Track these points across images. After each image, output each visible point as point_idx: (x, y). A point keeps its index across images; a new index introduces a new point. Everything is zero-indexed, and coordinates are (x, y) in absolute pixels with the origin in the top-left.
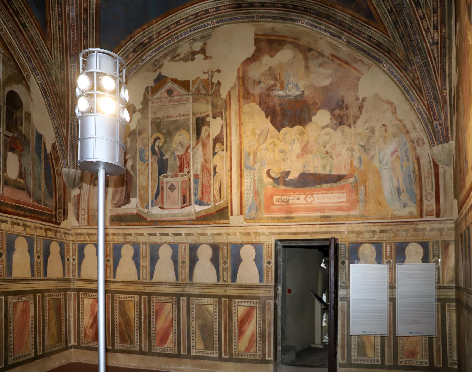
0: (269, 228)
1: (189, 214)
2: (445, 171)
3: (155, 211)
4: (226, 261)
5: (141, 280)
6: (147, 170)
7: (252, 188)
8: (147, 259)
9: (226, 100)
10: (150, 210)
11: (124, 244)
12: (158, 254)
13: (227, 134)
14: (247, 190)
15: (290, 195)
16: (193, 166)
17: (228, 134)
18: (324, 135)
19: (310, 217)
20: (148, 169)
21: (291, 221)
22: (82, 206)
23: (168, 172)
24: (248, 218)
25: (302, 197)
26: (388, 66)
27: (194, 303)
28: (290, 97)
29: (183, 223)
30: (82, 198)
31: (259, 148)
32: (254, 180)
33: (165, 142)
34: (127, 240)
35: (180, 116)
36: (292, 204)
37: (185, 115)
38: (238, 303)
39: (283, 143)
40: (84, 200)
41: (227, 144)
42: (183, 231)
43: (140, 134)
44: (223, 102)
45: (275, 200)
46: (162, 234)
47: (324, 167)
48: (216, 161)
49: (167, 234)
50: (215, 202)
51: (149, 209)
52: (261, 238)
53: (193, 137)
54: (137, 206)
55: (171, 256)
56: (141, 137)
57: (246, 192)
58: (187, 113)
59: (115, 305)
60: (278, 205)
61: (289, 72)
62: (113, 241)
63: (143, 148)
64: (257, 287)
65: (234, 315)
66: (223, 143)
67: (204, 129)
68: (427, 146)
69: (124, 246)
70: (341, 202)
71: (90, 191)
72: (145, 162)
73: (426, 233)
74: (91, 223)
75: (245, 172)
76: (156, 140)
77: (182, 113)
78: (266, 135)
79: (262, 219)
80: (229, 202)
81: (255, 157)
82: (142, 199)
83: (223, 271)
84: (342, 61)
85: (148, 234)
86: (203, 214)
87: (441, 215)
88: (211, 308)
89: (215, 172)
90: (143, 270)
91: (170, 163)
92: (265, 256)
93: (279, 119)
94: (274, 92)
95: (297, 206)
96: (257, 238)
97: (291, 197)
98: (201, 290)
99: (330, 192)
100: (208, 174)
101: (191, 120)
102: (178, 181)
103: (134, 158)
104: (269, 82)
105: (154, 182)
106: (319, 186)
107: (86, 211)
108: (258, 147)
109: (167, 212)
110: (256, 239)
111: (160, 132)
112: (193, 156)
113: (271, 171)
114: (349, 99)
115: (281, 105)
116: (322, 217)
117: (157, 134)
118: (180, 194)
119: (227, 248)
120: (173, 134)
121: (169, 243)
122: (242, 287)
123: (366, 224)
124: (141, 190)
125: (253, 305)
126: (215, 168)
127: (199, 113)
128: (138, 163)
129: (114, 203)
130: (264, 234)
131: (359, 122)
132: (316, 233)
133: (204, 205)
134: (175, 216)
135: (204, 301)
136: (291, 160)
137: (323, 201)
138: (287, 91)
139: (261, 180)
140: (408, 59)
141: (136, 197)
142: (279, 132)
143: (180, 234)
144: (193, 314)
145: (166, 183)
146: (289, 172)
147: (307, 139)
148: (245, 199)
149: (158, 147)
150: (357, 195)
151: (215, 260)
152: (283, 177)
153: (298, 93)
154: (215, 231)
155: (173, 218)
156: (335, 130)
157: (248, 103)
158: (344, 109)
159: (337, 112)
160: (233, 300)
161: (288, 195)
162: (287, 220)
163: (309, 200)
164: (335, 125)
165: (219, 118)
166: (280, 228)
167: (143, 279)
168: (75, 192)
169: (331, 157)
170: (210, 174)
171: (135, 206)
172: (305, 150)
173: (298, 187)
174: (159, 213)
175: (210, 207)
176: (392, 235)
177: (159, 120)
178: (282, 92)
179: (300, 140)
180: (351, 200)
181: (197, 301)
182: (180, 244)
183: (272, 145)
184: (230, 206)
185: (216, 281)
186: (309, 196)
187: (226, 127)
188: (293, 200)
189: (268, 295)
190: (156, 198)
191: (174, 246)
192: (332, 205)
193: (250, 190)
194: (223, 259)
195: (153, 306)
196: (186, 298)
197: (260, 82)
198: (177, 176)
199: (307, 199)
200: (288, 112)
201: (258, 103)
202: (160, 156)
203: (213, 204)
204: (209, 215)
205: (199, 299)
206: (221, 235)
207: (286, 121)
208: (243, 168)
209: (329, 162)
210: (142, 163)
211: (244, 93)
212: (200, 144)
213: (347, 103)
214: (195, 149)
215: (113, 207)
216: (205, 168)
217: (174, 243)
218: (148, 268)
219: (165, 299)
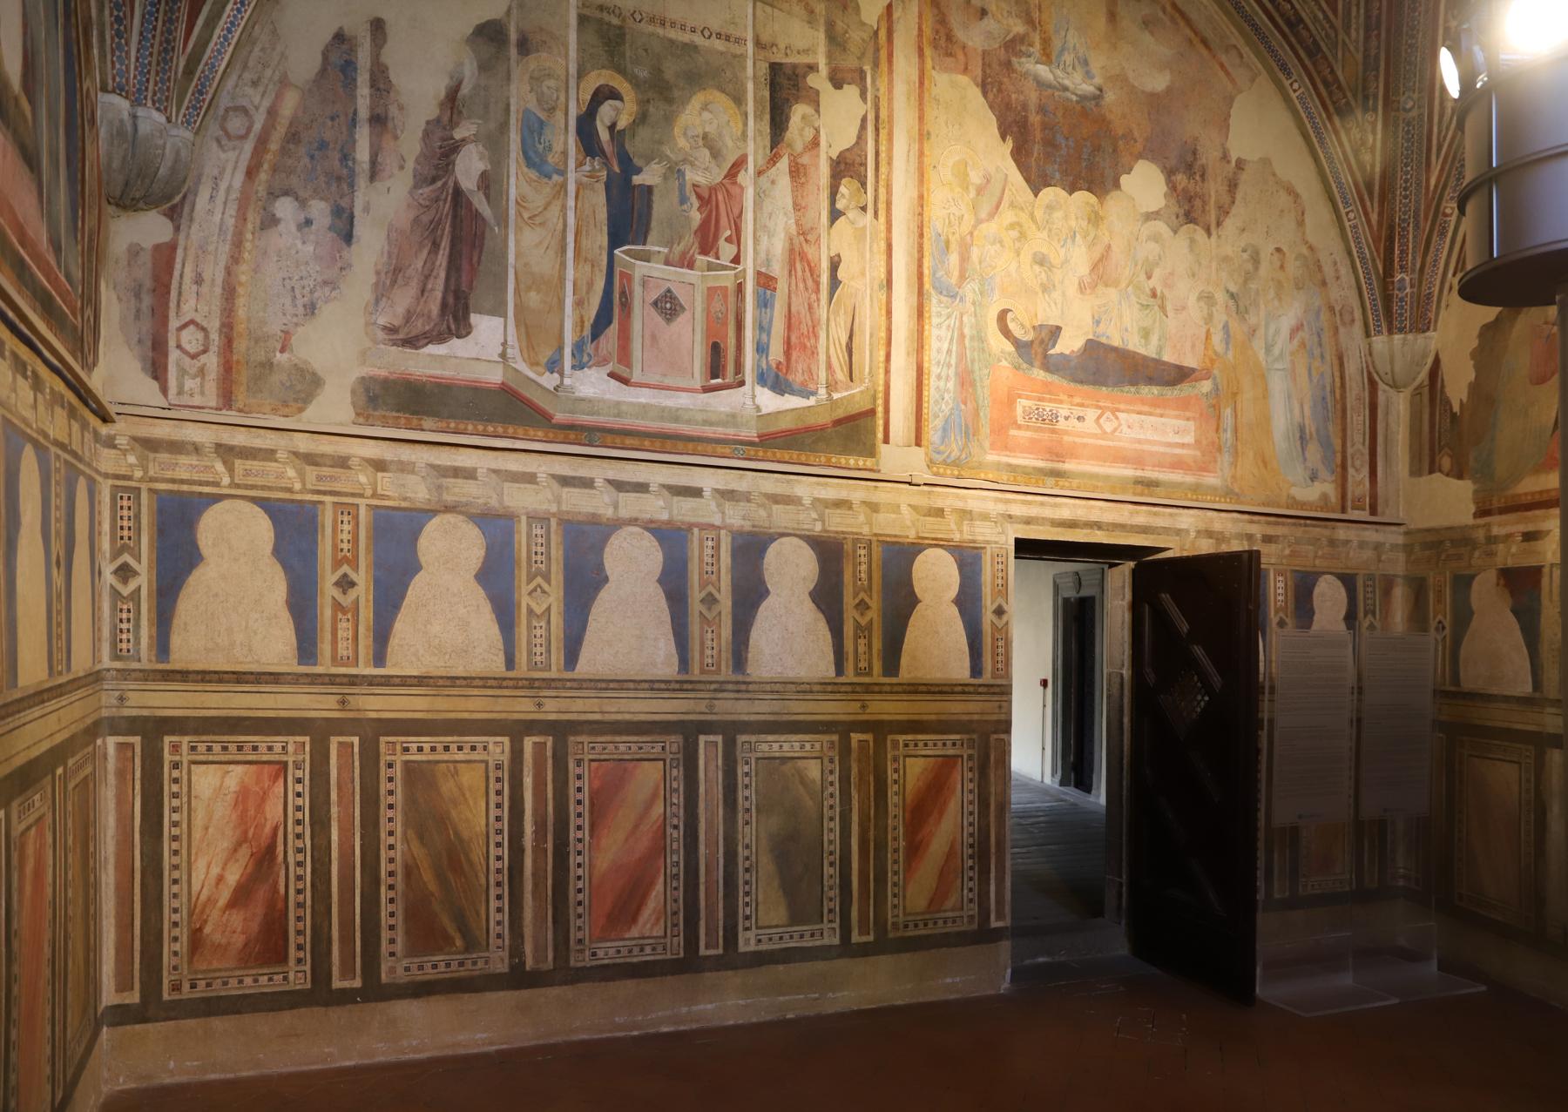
0: (1001, 500)
1: (732, 419)
2: (1388, 400)
3: (592, 385)
4: (867, 599)
5: (522, 670)
6: (555, 210)
7: (953, 362)
8: (549, 582)
9: (876, 33)
10: (567, 381)
11: (434, 513)
12: (600, 567)
13: (877, 154)
14: (939, 362)
15: (1061, 402)
17: (883, 155)
18: (1149, 238)
19: (1107, 478)
20: (564, 208)
21: (1061, 483)
22: (185, 307)
23: (650, 239)
24: (940, 458)
25: (1091, 414)
26: (1302, 90)
27: (753, 756)
28: (1068, 94)
29: (709, 448)
30: (184, 269)
31: (976, 233)
32: (962, 336)
33: (642, 119)
34: (449, 498)
35: (706, 32)
36: (1066, 432)
37: (728, 38)
38: (906, 745)
39: (1045, 234)
40: (199, 280)
41: (876, 190)
42: (708, 481)
43: (524, 46)
44: (865, 36)
45: (1019, 410)
46: (619, 486)
47: (1146, 334)
48: (839, 240)
49: (642, 488)
50: (831, 386)
51: (562, 375)
52: (977, 530)
53: (759, 132)
54: (503, 355)
55: (657, 575)
56: (532, 62)
57: (935, 370)
58: (732, 31)
59: (384, 787)
60: (1028, 428)
61: (1065, 11)
62: (375, 495)
63: (542, 116)
64: (964, 693)
65: (892, 789)
66: (864, 184)
67: (799, 112)
68: (1358, 329)
69: (433, 527)
70: (1183, 445)
71: (238, 244)
72: (550, 178)
73: (1351, 554)
74: (241, 397)
75: (934, 301)
76: (604, 94)
77: (715, 25)
78: (998, 194)
79: (980, 466)
80: (880, 395)
81: (964, 259)
82: (531, 330)
83: (857, 637)
84: (1196, 33)
85: (554, 476)
86: (785, 424)
87: (1380, 509)
88: (813, 770)
89: (835, 283)
90: (530, 628)
91: (660, 207)
92: (987, 591)
93: (1035, 155)
94: (1023, 60)
95: (1078, 440)
96: (965, 528)
97: (1063, 411)
98: (777, 706)
99: (1158, 411)
100: (810, 283)
101: (750, 63)
102: (693, 284)
103: (495, 144)
104: (1011, 21)
105: (588, 268)
106: (1133, 389)
107: (215, 336)
108: (975, 227)
109: (643, 400)
110: (961, 532)
111: (621, 71)
112: (758, 205)
113: (1010, 315)
114: (1209, 155)
115: (1042, 109)
116: (1139, 482)
117: (604, 72)
118: (699, 337)
119: (870, 555)
120: (676, 93)
121: (652, 521)
122: (916, 692)
123: (1235, 515)
124: (529, 289)
125: (951, 752)
126: (835, 265)
127: (782, 46)
128: (513, 170)
129: (382, 321)
130: (985, 517)
131: (1230, 224)
132: (1122, 527)
133: (792, 393)
134: (677, 420)
135: (788, 745)
136: (1064, 294)
137: (1142, 437)
138: (1059, 73)
139: (980, 338)
140: (1365, 88)
141: (505, 317)
142: (1036, 196)
143: (696, 492)
144: (747, 795)
145: (644, 284)
146: (1059, 329)
147: (1106, 239)
148: (930, 393)
149: (612, 127)
150: (1217, 430)
151: (827, 597)
152: (1042, 342)
153: (1088, 88)
154: (832, 490)
155: (671, 427)
156: (1175, 232)
157: (946, 70)
158: (1198, 178)
159: (1180, 178)
160: (890, 737)
161: (1055, 401)
162: (1051, 481)
163: (1108, 427)
164: (1174, 217)
165: (851, 91)
166: (1030, 503)
167: (533, 666)
168: (149, 228)
169: (1163, 308)
170: (817, 284)
171: (494, 352)
172: (1100, 273)
173: (1081, 382)
174: (607, 396)
175: (812, 401)
176: (1287, 552)
177: (615, 21)
178: (1047, 68)
179: (1090, 238)
180: (1204, 442)
181: (765, 747)
182: (696, 531)
183: (1014, 234)
184: (880, 410)
185: (831, 672)
186: (1108, 414)
187: (877, 129)
188: (1067, 418)
189: (995, 717)
190: (595, 336)
191: (671, 538)
192: (1162, 449)
193: (949, 365)
194: (856, 595)
195: (579, 777)
196: (719, 739)
197: (983, 13)
198: (691, 266)
199: (1102, 421)
200: (1060, 140)
201: (980, 80)
202: (617, 169)
203: (822, 391)
204: (808, 430)
205: (770, 738)
206: (850, 508)
207: (1056, 167)
208: (927, 286)
209: (1157, 324)
210: (533, 174)
211: (937, 32)
212: (784, 163)
213: (1204, 161)
214: (763, 179)
215: (375, 342)
216: (796, 256)
217: (669, 522)
218: (556, 620)
219: (634, 747)
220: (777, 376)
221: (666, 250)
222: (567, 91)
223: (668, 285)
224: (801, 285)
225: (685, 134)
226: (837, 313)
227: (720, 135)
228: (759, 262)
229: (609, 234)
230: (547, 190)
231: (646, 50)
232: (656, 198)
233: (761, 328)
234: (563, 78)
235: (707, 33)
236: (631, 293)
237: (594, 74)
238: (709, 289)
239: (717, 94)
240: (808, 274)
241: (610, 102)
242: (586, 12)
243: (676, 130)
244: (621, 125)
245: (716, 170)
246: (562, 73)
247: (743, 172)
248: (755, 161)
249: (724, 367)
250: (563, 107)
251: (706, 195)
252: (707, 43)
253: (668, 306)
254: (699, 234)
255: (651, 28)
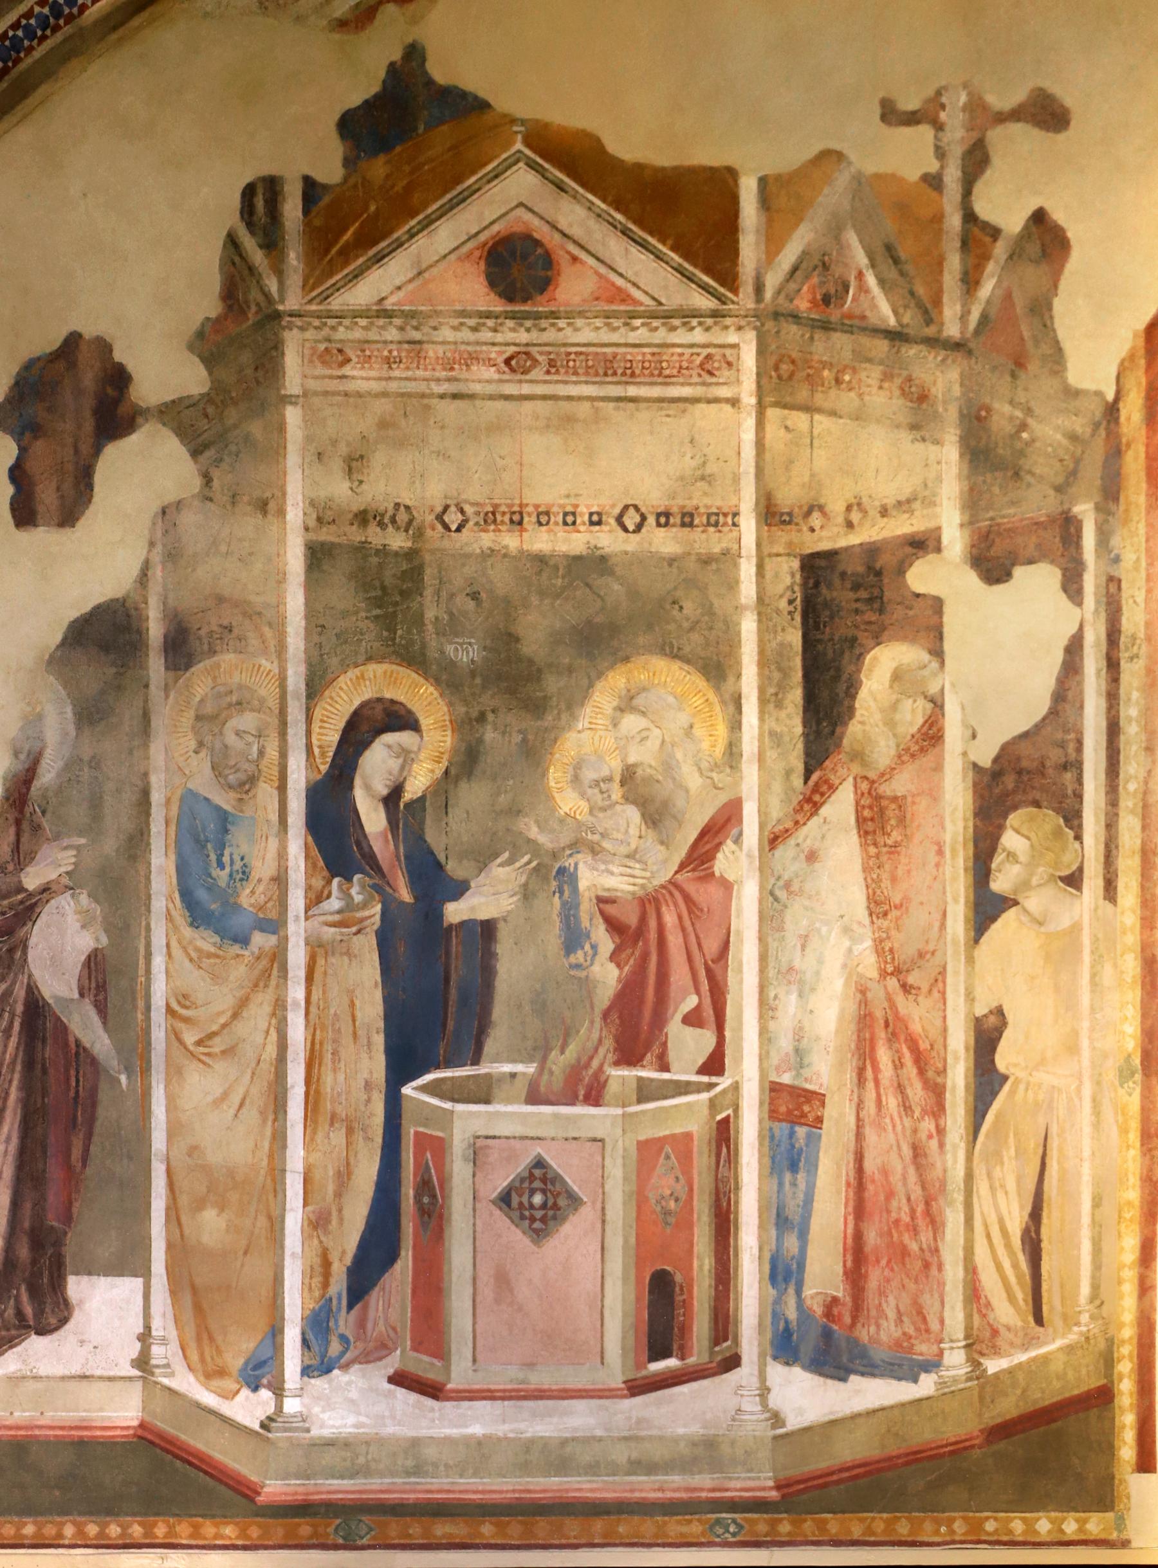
16: (766, 1007)
23: (490, 1047)
41: (1111, 826)
66: (1073, 818)
117: (375, 669)
118: (616, 1264)
120: (552, 684)
149: (392, 799)
177: (398, 541)
198: (594, 1096)
202: (405, 895)
214: (785, 853)
220: (827, 1334)
221: (531, 1069)
222: (283, 734)
223: (538, 1149)
224: (892, 1102)
225: (576, 779)
226: (995, 1157)
227: (668, 766)
228: (775, 1059)
229: (389, 1051)
230: (239, 972)
231: (475, 596)
232: (504, 947)
233: (782, 1222)
234: (273, 703)
235: (631, 520)
236: (444, 1181)
237: (344, 681)
238: (643, 1146)
239: (660, 664)
240: (910, 1070)
241: (389, 738)
242: (326, 535)
243: (556, 776)
244: (417, 784)
245: (655, 852)
246: (268, 692)
247: (729, 846)
248: (763, 814)
249: (685, 1329)
250: (275, 771)
251: (632, 920)
252: (631, 544)
253: (538, 1199)
254: (615, 1016)
255: (487, 539)
